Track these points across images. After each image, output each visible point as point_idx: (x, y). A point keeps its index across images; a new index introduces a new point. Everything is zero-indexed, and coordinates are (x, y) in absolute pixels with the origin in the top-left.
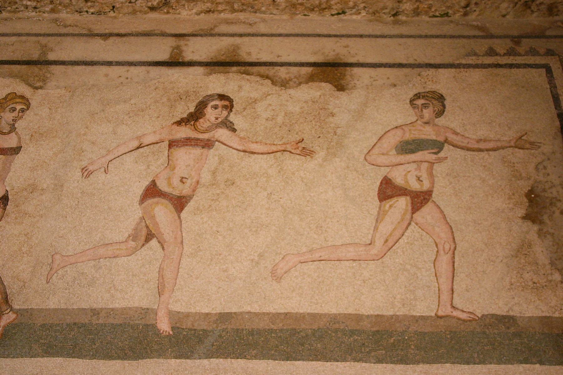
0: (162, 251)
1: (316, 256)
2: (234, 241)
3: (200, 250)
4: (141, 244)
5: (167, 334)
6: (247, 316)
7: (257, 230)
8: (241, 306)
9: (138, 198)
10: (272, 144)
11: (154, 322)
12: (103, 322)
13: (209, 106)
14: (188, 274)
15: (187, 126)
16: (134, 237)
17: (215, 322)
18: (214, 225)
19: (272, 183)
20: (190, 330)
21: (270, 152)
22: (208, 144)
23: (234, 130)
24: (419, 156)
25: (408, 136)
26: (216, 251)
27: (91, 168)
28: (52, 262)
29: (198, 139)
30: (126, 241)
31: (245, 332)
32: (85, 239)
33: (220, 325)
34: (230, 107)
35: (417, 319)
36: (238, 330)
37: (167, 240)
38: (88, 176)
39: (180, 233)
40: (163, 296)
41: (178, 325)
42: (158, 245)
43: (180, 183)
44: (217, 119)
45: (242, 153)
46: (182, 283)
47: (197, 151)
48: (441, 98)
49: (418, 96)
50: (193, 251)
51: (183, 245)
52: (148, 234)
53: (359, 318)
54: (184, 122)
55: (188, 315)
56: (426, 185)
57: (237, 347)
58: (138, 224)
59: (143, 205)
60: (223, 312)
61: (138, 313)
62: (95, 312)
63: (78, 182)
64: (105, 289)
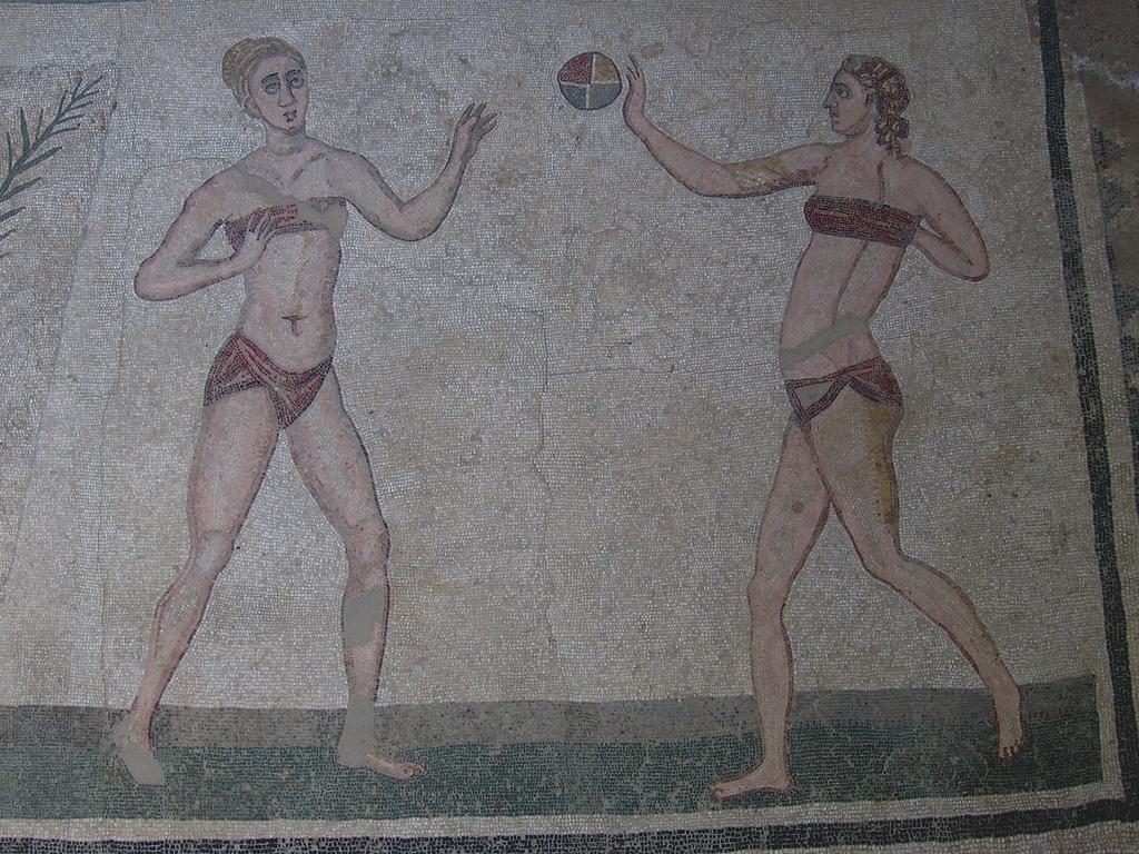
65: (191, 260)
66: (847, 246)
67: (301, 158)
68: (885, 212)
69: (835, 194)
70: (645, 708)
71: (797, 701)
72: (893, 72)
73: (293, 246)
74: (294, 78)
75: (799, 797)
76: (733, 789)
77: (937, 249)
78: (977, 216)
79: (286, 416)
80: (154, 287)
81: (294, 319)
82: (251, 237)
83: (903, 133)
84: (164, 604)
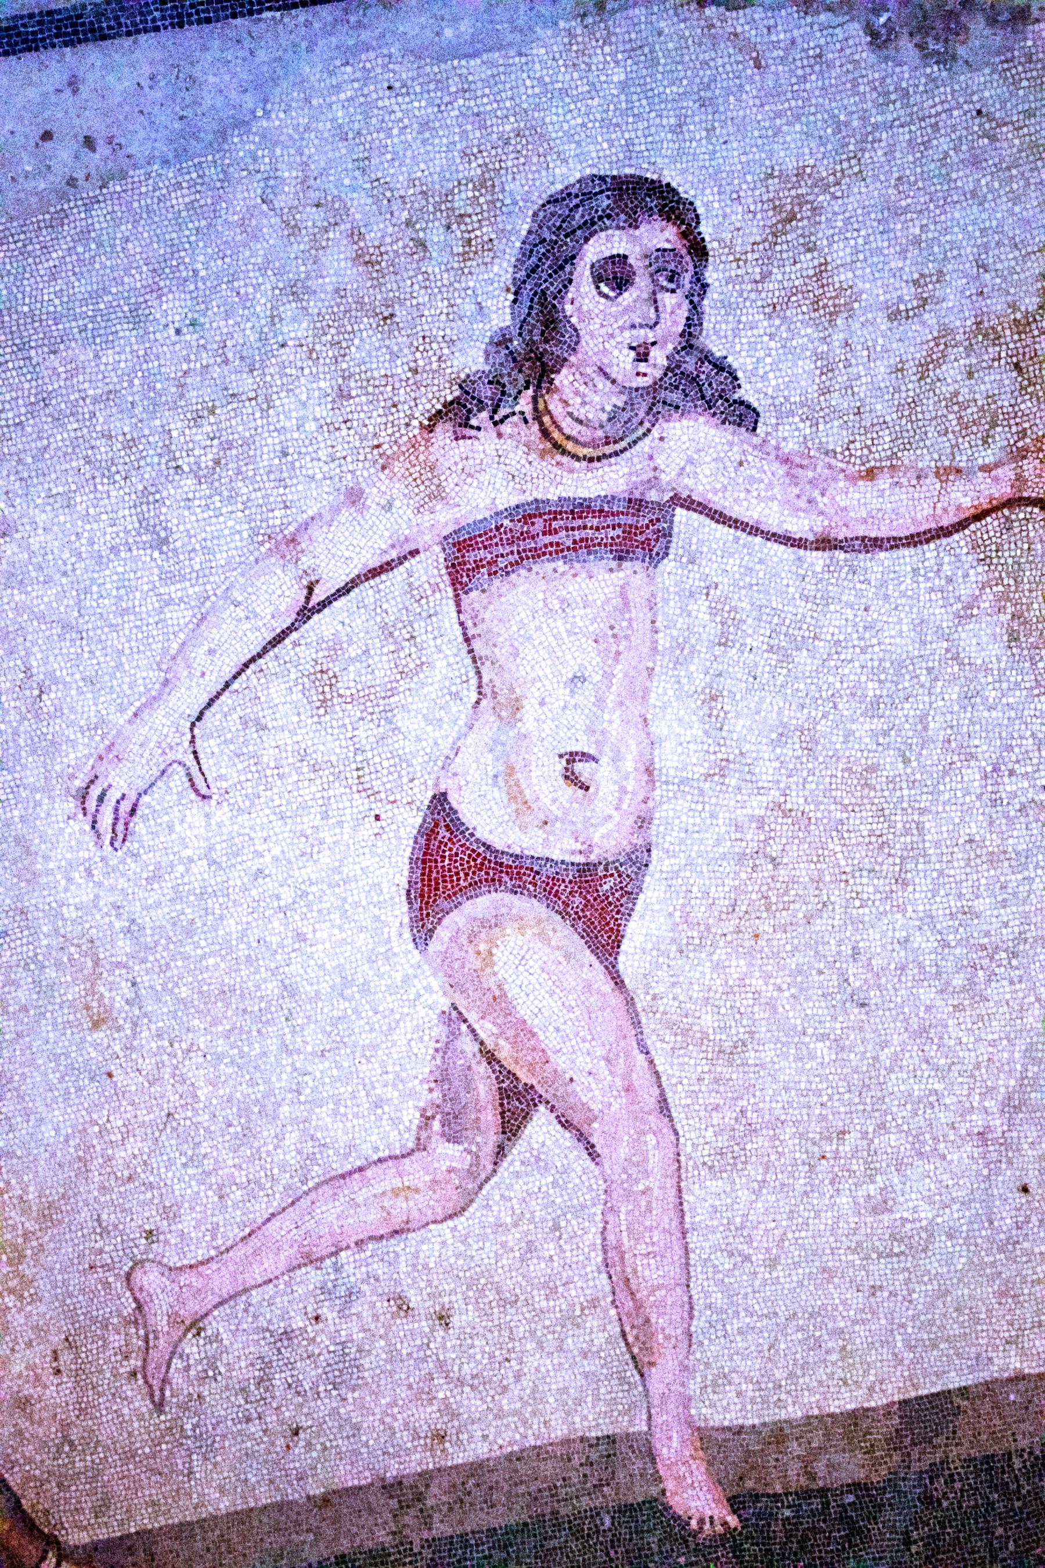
0: (592, 1166)
2: (885, 1055)
3: (752, 1130)
4: (490, 1148)
5: (719, 1529)
6: (1012, 1397)
7: (972, 981)
8: (978, 1357)
9: (400, 912)
10: (948, 470)
11: (654, 1491)
12: (450, 1531)
13: (582, 273)
14: (731, 1255)
15: (506, 428)
17: (895, 1441)
18: (780, 989)
19: (990, 709)
20: (805, 1494)
21: (945, 522)
26: (823, 1118)
28: (139, 1307)
29: (581, 509)
30: (421, 1146)
31: (1017, 1463)
32: (239, 1167)
33: (915, 1455)
36: (988, 1459)
37: (596, 1107)
38: (120, 827)
39: (641, 1057)
40: (654, 1370)
41: (750, 1484)
42: (566, 1138)
43: (570, 791)
44: (642, 356)
45: (817, 559)
46: (718, 1298)
50: (722, 1141)
51: (671, 1119)
52: (504, 1094)
54: (481, 406)
57: (1000, 1531)
58: (444, 1050)
59: (434, 946)
60: (913, 1394)
61: (576, 1461)
63: (89, 872)
64: (410, 1387)
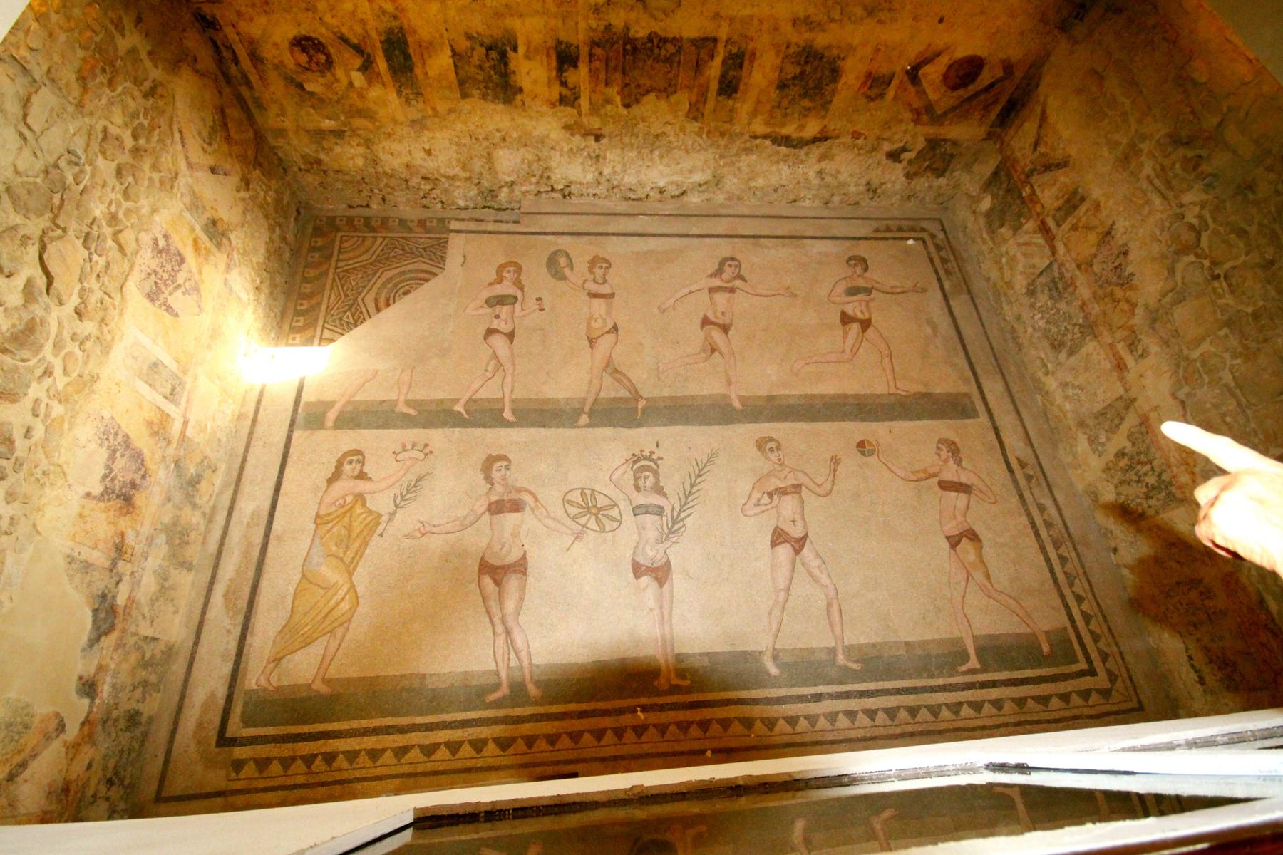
1: (814, 360)
16: (704, 351)
22: (732, 290)
23: (746, 281)
24: (858, 297)
25: (850, 285)
27: (664, 306)
34: (739, 266)
35: (878, 396)
47: (727, 295)
48: (864, 260)
49: (850, 259)
53: (846, 396)
55: (749, 398)
56: (867, 316)
62: (693, 398)
65: (757, 504)
66: (953, 494)
67: (786, 472)
68: (961, 484)
69: (946, 479)
70: (927, 642)
71: (975, 638)
72: (953, 443)
73: (788, 498)
74: (778, 448)
75: (984, 670)
76: (963, 668)
77: (980, 495)
78: (989, 483)
79: (797, 552)
80: (748, 513)
81: (793, 521)
82: (775, 497)
83: (961, 460)
84: (770, 614)
